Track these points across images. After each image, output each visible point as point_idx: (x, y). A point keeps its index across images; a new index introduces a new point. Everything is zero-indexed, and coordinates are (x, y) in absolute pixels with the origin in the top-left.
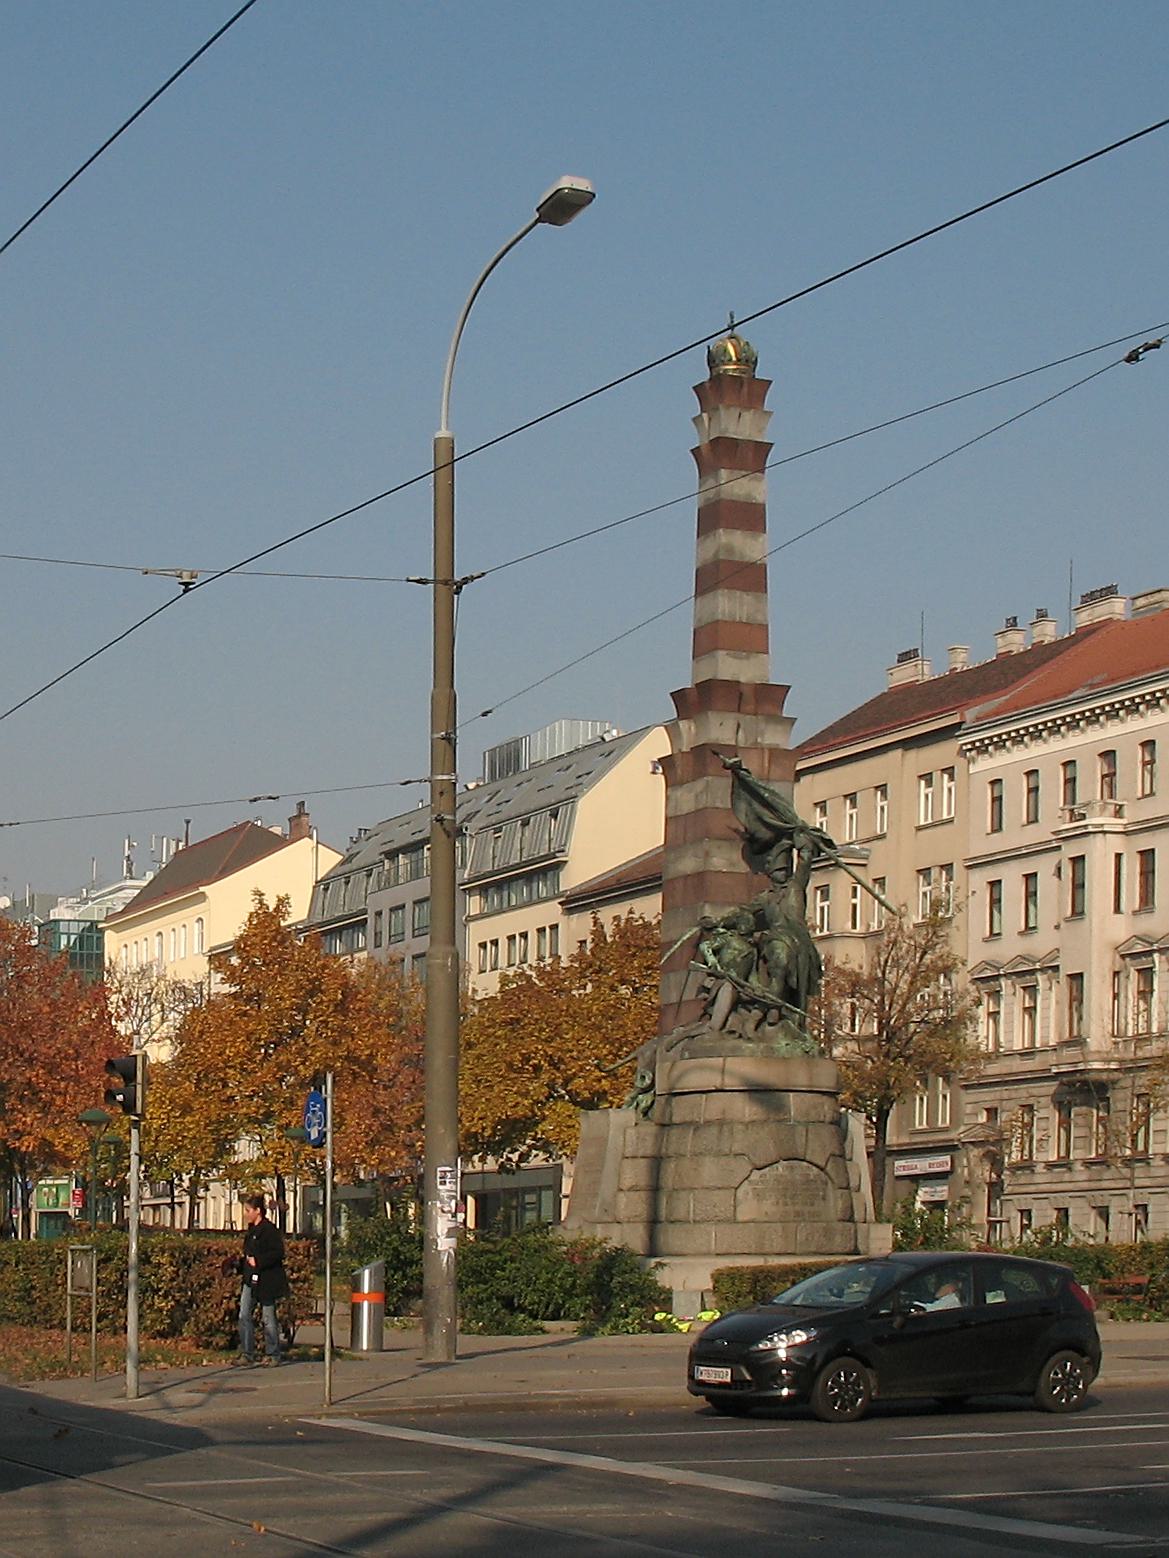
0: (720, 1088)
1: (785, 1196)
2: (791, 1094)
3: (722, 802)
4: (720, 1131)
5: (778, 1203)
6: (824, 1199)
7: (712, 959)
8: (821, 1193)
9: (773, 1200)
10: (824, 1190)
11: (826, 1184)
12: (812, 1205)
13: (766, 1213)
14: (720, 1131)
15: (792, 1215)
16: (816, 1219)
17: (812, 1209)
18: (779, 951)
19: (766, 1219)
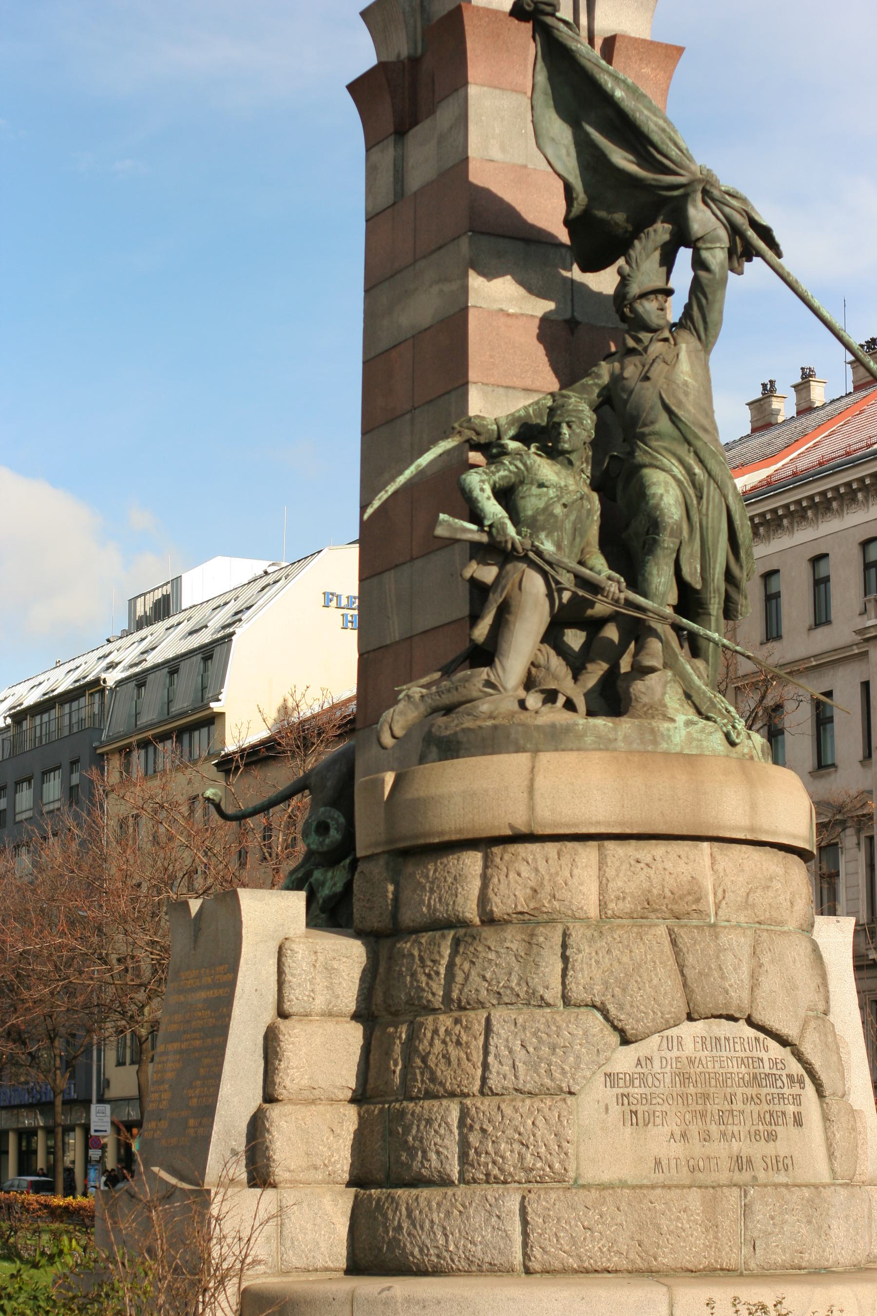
0: (524, 830)
1: (703, 1115)
2: (706, 845)
3: (503, 149)
4: (530, 943)
5: (684, 1135)
6: (798, 1121)
7: (493, 509)
8: (791, 1109)
9: (673, 1125)
10: (797, 1099)
11: (801, 1082)
12: (771, 1137)
13: (658, 1163)
14: (530, 943)
15: (725, 1164)
16: (782, 1178)
17: (770, 1149)
18: (660, 490)
19: (659, 1177)
